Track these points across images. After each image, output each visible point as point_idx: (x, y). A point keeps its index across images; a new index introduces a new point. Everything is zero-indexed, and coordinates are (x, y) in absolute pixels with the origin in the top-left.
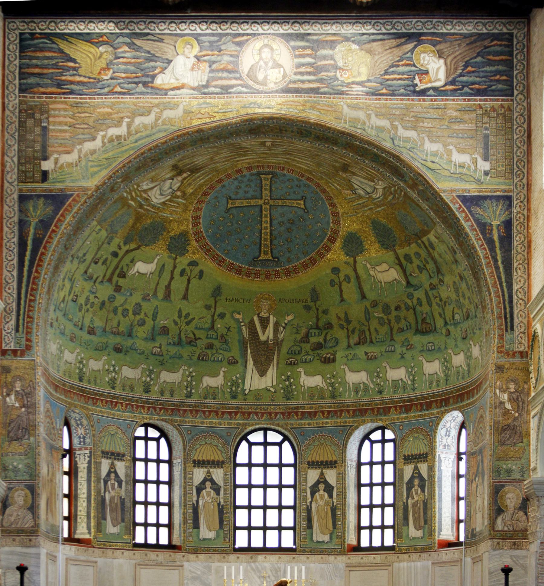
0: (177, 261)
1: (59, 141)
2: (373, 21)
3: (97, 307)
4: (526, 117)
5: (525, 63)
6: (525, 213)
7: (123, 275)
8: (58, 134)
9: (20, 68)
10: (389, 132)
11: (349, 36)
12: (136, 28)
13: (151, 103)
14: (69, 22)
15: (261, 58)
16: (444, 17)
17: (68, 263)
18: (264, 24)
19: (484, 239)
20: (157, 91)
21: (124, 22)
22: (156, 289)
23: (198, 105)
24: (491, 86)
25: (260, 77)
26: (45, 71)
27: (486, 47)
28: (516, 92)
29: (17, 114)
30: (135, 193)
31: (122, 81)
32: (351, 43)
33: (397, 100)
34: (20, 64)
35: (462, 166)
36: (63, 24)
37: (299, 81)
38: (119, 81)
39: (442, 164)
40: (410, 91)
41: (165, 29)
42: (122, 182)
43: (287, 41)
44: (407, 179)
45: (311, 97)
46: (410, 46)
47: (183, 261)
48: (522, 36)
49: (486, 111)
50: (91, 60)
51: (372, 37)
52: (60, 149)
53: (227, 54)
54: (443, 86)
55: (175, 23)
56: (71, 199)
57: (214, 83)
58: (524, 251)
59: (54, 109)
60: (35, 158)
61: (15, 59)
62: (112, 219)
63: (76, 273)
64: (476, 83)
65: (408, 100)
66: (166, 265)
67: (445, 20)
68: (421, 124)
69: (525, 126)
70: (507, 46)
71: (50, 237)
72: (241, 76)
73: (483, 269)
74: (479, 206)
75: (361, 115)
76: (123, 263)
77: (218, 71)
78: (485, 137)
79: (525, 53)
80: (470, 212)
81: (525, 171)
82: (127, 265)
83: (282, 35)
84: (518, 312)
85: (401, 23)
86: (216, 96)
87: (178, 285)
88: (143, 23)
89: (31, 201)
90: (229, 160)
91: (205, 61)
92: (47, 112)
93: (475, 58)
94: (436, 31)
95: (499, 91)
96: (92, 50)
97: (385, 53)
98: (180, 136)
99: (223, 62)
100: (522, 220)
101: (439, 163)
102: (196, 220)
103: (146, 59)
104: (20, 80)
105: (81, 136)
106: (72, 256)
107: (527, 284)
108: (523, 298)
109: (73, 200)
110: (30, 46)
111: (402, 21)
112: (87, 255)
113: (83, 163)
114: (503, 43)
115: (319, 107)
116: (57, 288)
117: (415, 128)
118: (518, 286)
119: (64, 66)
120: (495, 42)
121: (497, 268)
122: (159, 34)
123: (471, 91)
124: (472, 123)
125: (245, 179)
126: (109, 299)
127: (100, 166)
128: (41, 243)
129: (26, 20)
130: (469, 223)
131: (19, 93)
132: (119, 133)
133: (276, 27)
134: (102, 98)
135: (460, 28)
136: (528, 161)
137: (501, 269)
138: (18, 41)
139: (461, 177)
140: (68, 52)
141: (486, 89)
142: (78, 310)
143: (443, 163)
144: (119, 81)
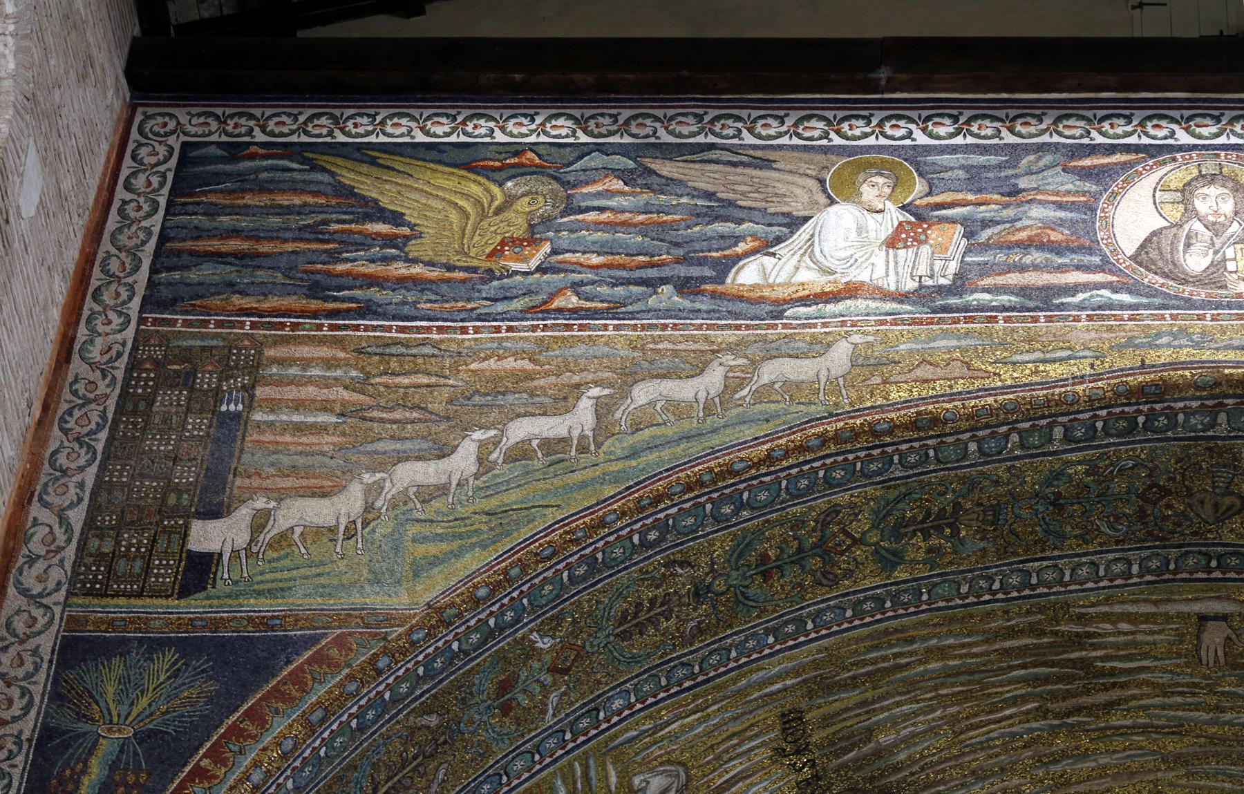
1: (286, 461)
8: (288, 438)
9: (163, 238)
13: (707, 339)
14: (391, 117)
15: (1190, 212)
18: (1198, 120)
20: (738, 307)
25: (1196, 262)
26: (265, 247)
29: (120, 375)
36: (365, 120)
53: (1041, 202)
56: (308, 654)
57: (988, 281)
59: (280, 362)
60: (163, 510)
61: (149, 215)
86: (1001, 316)
88: (691, 120)
89: (116, 661)
91: (951, 220)
92: (254, 369)
96: (475, 189)
98: (837, 437)
103: (698, 215)
104: (154, 270)
109: (309, 661)
110: (218, 177)
113: (382, 529)
119: (351, 232)
122: (755, 147)
127: (460, 536)
129: (219, 111)
132: (564, 433)
134: (498, 329)
140: (374, 195)
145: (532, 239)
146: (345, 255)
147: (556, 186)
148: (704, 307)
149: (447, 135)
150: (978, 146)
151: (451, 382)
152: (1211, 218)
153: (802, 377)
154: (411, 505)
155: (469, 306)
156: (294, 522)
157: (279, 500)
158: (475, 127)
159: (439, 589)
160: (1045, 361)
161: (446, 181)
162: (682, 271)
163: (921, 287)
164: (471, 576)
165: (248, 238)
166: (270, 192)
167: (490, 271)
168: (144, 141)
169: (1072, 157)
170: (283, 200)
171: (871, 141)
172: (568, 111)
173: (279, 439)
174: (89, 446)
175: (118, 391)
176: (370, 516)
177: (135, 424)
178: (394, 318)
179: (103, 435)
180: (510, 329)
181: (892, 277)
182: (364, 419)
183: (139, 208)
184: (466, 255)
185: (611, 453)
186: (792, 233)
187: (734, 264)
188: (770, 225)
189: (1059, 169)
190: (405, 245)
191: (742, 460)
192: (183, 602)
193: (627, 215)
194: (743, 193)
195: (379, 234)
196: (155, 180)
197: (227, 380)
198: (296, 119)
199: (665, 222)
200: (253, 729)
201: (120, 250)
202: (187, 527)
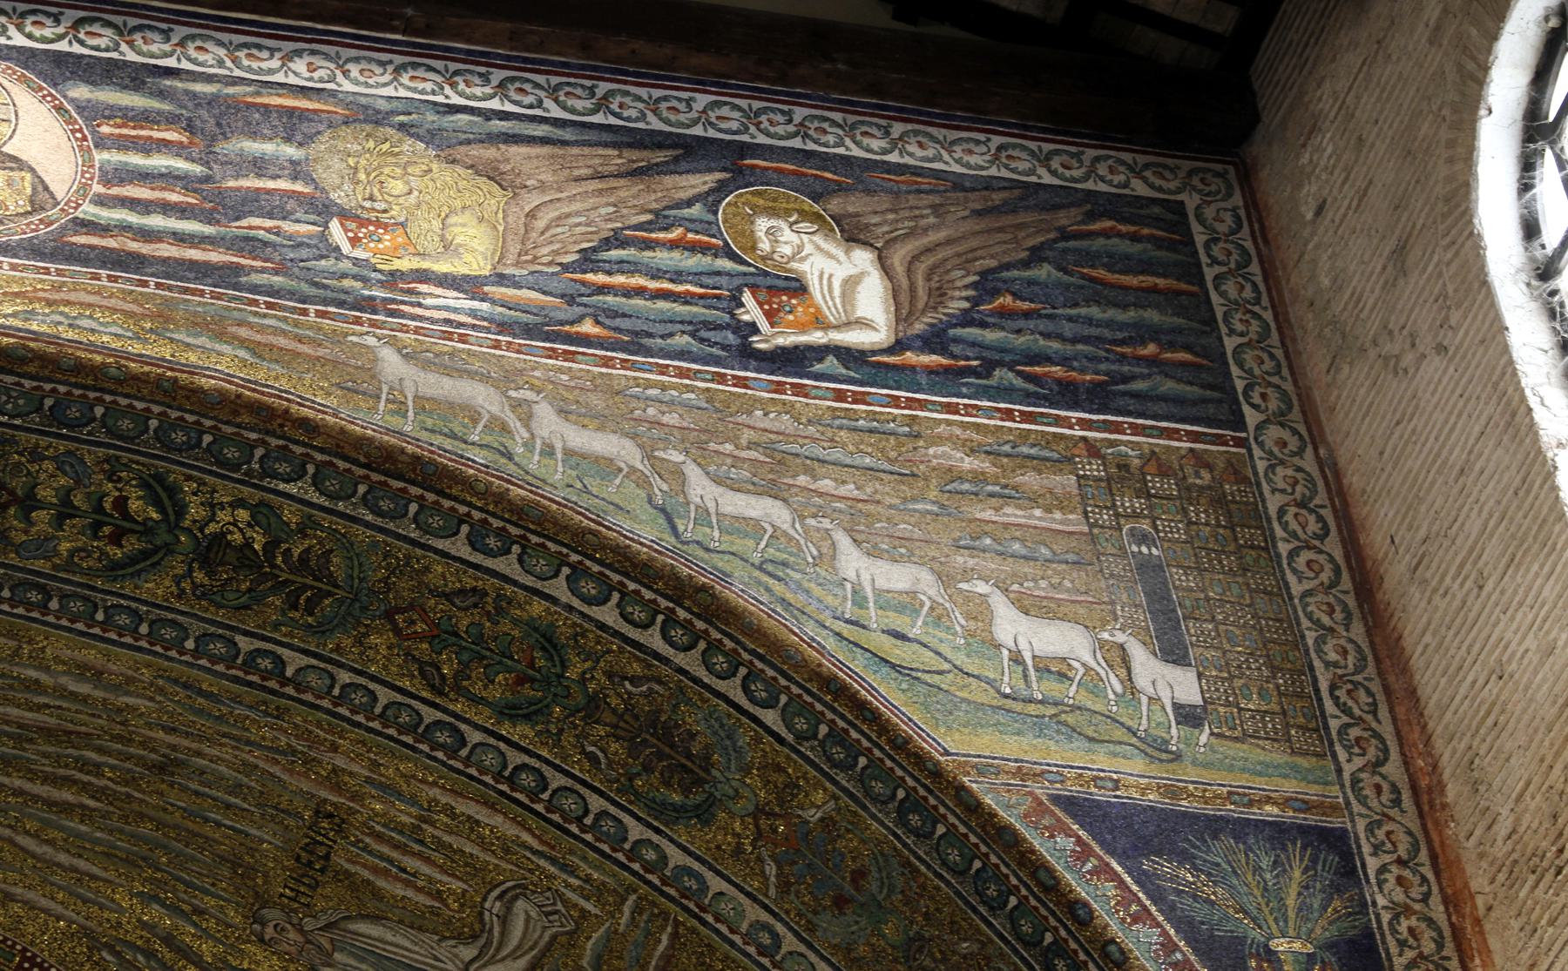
2: (498, 75)
4: (1327, 513)
5: (1268, 316)
6: (1438, 910)
11: (382, 105)
16: (846, 106)
24: (1126, 379)
27: (1065, 235)
28: (1251, 417)
32: (390, 131)
33: (663, 370)
37: (125, 228)
40: (724, 347)
45: (202, 293)
48: (1228, 218)
49: (1124, 467)
51: (498, 125)
54: (890, 350)
64: (1047, 359)
65: (721, 379)
67: (852, 119)
68: (802, 480)
69: (1333, 546)
70: (1172, 246)
75: (484, 398)
79: (1259, 279)
81: (1387, 730)
83: (24, 58)
93: (1026, 264)
94: (811, 146)
95: (1164, 398)
97: (576, 189)
100: (1428, 947)
101: (934, 643)
111: (643, 92)
114: (1146, 231)
115: (243, 332)
117: (774, 491)
120: (1108, 224)
123: (1031, 387)
135: (930, 153)
141: (1101, 384)
143: (953, 645)
172: (106, 16)
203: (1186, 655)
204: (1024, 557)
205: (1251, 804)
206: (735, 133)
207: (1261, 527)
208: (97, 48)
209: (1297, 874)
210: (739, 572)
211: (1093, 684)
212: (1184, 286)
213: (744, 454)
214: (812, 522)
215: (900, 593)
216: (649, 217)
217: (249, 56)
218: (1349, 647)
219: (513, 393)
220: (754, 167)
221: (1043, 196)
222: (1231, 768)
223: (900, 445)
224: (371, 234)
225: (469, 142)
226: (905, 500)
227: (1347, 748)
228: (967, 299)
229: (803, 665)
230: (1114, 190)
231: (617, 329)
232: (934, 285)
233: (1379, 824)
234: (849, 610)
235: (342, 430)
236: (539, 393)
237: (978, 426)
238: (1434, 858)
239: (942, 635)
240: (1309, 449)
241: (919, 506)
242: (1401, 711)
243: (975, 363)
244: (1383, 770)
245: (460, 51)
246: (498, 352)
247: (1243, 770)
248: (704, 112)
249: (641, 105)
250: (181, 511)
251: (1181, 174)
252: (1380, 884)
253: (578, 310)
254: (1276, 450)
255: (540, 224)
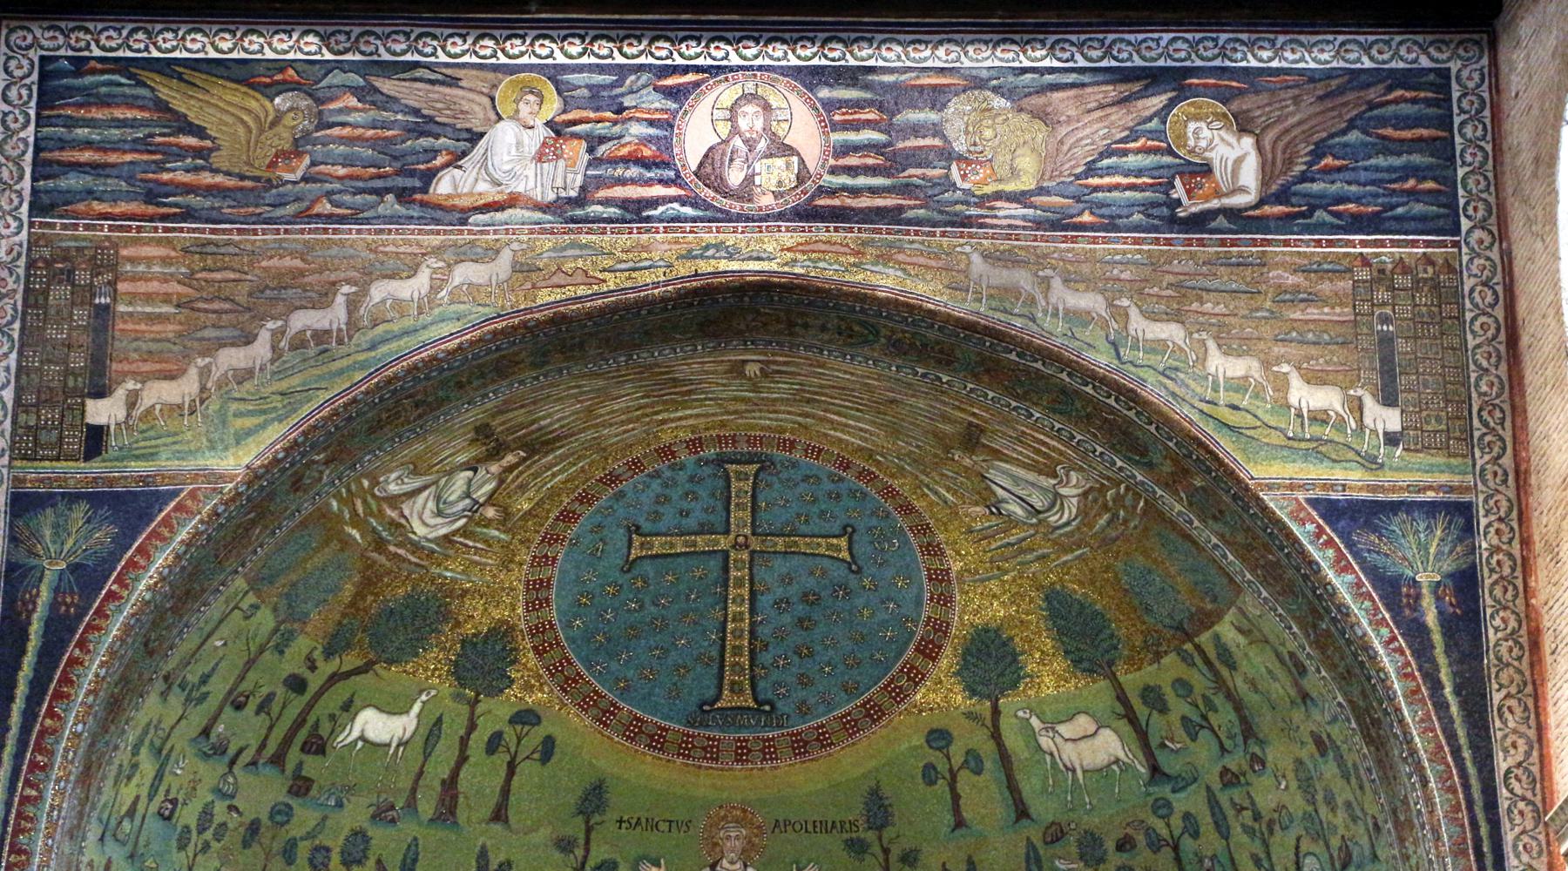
0: (480, 708)
1: (144, 346)
3: (233, 838)
4: (1499, 289)
5: (1489, 148)
6: (1516, 548)
7: (317, 746)
8: (143, 327)
10: (1105, 325)
11: (984, 74)
12: (382, 50)
13: (419, 244)
14: (189, 32)
15: (735, 131)
17: (152, 702)
18: (745, 42)
19: (1395, 623)
20: (439, 214)
21: (348, 34)
22: (414, 790)
23: (554, 249)
24: (1393, 207)
25: (735, 177)
26: (113, 158)
27: (1372, 106)
28: (1465, 224)
29: (21, 271)
30: (365, 502)
31: (337, 186)
32: (989, 93)
34: (36, 139)
35: (1320, 418)
36: (169, 35)
37: (844, 188)
38: (328, 186)
39: (1260, 413)
40: (1161, 218)
41: (464, 53)
42: (327, 463)
43: (811, 88)
44: (1156, 458)
45: (879, 231)
46: (1157, 102)
47: (496, 712)
48: (1476, 76)
49: (1381, 271)
50: (249, 131)
51: (1049, 78)
52: (146, 367)
53: (638, 120)
55: (493, 37)
56: (173, 504)
57: (602, 194)
58: (1519, 659)
59: (132, 260)
60: (68, 393)
61: (25, 126)
62: (294, 577)
63: (177, 732)
65: (1157, 241)
66: (445, 719)
68: (1195, 306)
69: (1499, 312)
71: (100, 613)
72: (678, 176)
73: (1398, 710)
74: (1376, 529)
75: (1023, 279)
76: (320, 711)
77: (614, 161)
78: (1381, 341)
79: (1488, 121)
80: (1350, 545)
82: (332, 717)
84: (1517, 838)
85: (1129, 43)
87: (482, 777)
88: (401, 38)
89: (49, 511)
90: (638, 419)
92: (113, 267)
93: (1344, 132)
94: (1228, 63)
95: (1414, 218)
96: (253, 104)
99: (627, 139)
100: (1507, 571)
101: (1252, 408)
102: (537, 592)
103: (409, 131)
104: (34, 179)
105: (210, 333)
106: (166, 678)
107: (1535, 753)
108: (1529, 795)
109: (176, 509)
110: (71, 90)
111: (1131, 37)
112: (213, 679)
114: (1422, 95)
115: (901, 257)
116: (114, 769)
117: (1177, 317)
118: (1511, 762)
119: (170, 145)
120: (1399, 93)
121: (1441, 706)
122: (447, 65)
124: (1341, 305)
125: (682, 476)
126: (271, 817)
128: (73, 631)
129: (63, 24)
130: (1350, 578)
131: (30, 216)
132: (327, 326)
133: (778, 50)
134: (277, 232)
135: (1297, 56)
136: (1513, 408)
137: (1454, 709)
138: (35, 77)
139: (1318, 450)
140: (183, 110)
141: (1377, 214)
142: (174, 844)
143: (1264, 412)
144: (328, 186)
145: (296, 151)
146: (168, 165)
147: (310, 102)
148: (415, 214)
149: (231, 51)
150: (598, 65)
151: (249, 277)
152: (748, 135)
153: (481, 281)
154: (230, 386)
155: (258, 211)
156: (153, 401)
157: (143, 382)
158: (251, 43)
159: (254, 454)
160: (634, 270)
161: (230, 95)
162: (401, 182)
163: (558, 198)
164: (273, 444)
165: (99, 149)
166: (109, 105)
167: (269, 181)
168: (11, 54)
169: (659, 78)
170: (119, 113)
171: (525, 60)
173: (137, 327)
174: (9, 336)
175: (22, 287)
176: (205, 396)
177: (38, 315)
178: (207, 221)
179: (17, 325)
180: (286, 231)
181: (539, 189)
182: (193, 309)
183: (16, 120)
184: (252, 166)
185: (358, 345)
186: (473, 147)
187: (435, 175)
188: (458, 140)
189: (651, 88)
190: (209, 156)
191: (443, 351)
192: (88, 465)
193: (360, 131)
194: (439, 110)
195: (190, 147)
196: (24, 92)
197: (97, 276)
198: (120, 34)
199: (386, 137)
200: (142, 562)
201: (7, 159)
202: (83, 404)
203: (1397, 400)
204: (1314, 343)
205: (1419, 492)
206: (1183, 60)
207: (1458, 303)
208: (833, 60)
209: (1439, 533)
210: (1151, 377)
211: (1341, 424)
212: (1441, 134)
213: (1164, 293)
214: (1196, 336)
215: (1239, 378)
216: (1126, 133)
217: (915, 49)
218: (1496, 381)
219: (1041, 273)
220: (1190, 85)
221: (1363, 77)
222: (1411, 470)
223: (1253, 272)
224: (973, 169)
225: (1030, 94)
226: (1252, 311)
227: (1482, 449)
228: (1305, 163)
229: (1182, 429)
230: (1409, 66)
231: (1102, 216)
232: (1287, 156)
233: (1492, 496)
234: (1209, 395)
235: (949, 315)
236: (1054, 269)
237: (1299, 253)
238: (1520, 514)
239: (1259, 404)
240: (1497, 244)
241: (1259, 314)
242: (1519, 421)
243: (1304, 208)
244: (1500, 462)
245: (1030, 24)
246: (1036, 244)
247: (1418, 470)
248: (1167, 47)
249: (1130, 48)
250: (878, 332)
251: (1452, 46)
252: (1486, 534)
253: (1081, 206)
254: (1476, 247)
255: (1065, 148)
